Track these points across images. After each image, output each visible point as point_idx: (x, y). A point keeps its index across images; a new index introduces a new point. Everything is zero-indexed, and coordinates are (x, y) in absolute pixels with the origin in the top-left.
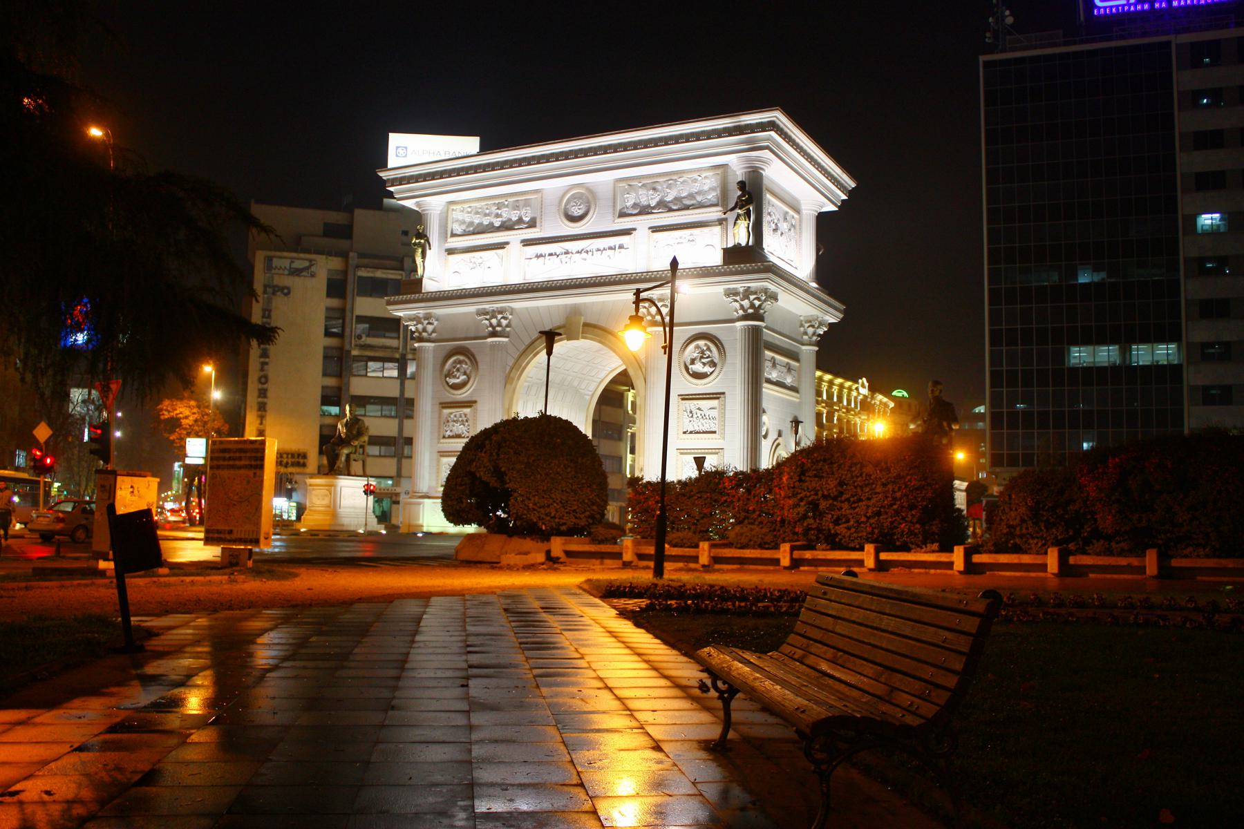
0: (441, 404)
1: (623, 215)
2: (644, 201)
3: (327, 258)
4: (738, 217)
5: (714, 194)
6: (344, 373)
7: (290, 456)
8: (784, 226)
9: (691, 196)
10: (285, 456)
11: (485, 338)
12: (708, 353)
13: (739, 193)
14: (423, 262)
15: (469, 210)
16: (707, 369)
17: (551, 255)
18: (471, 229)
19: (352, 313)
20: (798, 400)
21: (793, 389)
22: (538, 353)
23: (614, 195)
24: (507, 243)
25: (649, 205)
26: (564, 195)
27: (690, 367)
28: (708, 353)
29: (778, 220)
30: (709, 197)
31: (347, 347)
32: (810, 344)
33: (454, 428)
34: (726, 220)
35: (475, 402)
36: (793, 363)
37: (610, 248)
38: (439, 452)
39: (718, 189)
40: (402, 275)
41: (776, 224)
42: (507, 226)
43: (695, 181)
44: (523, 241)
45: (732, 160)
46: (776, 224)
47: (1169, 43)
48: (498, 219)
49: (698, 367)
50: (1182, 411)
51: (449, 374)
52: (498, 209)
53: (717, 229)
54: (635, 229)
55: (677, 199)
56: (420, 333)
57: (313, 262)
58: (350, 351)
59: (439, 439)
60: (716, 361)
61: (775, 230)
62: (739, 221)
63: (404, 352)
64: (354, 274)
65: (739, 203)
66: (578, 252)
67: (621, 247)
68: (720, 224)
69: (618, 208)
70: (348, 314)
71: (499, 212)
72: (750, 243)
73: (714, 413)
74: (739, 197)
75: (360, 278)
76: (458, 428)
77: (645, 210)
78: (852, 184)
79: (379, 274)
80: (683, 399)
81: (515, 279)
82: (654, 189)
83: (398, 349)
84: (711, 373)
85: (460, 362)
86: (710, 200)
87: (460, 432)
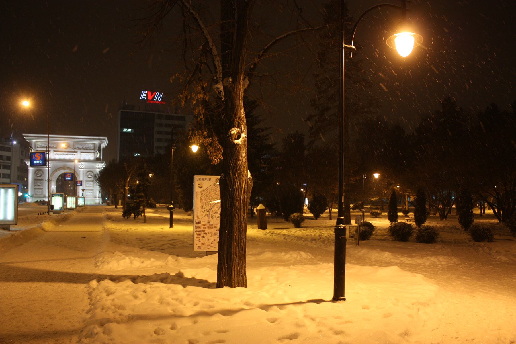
1: (75, 149)
2: (79, 147)
4: (98, 153)
9: (88, 147)
16: (91, 177)
18: (42, 147)
43: (89, 145)
45: (97, 143)
49: (89, 176)
51: (37, 174)
53: (93, 154)
55: (86, 148)
69: (74, 147)
73: (92, 184)
76: (39, 184)
77: (79, 149)
82: (81, 145)
85: (39, 172)
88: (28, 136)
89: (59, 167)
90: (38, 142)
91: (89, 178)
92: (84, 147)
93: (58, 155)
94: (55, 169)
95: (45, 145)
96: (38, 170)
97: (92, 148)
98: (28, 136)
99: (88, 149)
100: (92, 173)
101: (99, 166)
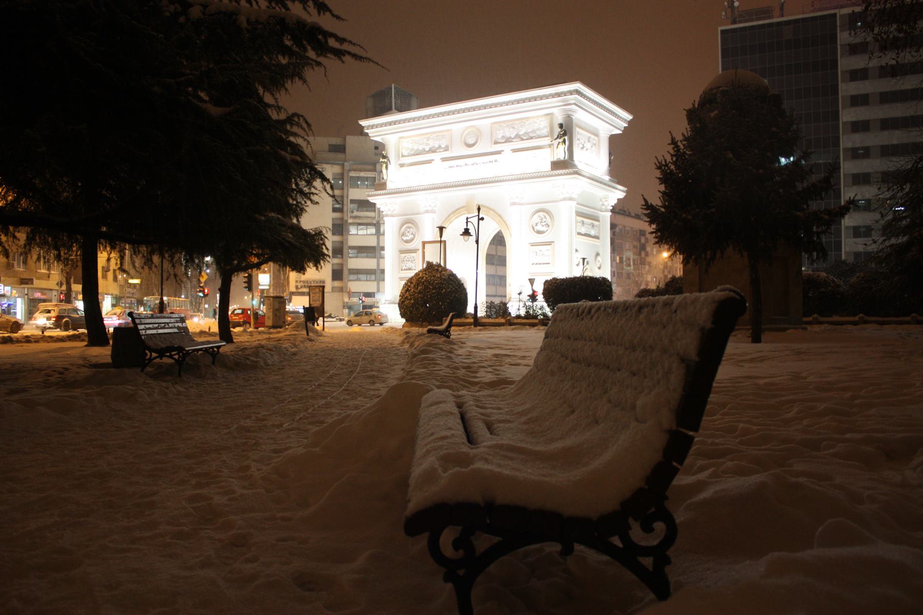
0: (400, 251)
1: (496, 143)
2: (508, 135)
3: (332, 167)
4: (559, 143)
5: (546, 130)
6: (344, 233)
7: (315, 282)
8: (588, 145)
9: (534, 131)
10: (312, 282)
11: (423, 214)
12: (544, 220)
13: (560, 130)
14: (387, 172)
15: (412, 141)
17: (457, 166)
18: (413, 152)
19: (348, 198)
20: (599, 244)
21: (597, 237)
22: (452, 221)
23: (491, 133)
24: (433, 160)
25: (511, 137)
26: (463, 132)
27: (535, 227)
28: (544, 220)
29: (584, 142)
30: (544, 132)
31: (345, 218)
32: (606, 211)
33: (407, 265)
34: (553, 144)
35: (418, 250)
36: (595, 223)
37: (490, 162)
38: (399, 278)
39: (548, 127)
40: (375, 175)
41: (583, 145)
42: (432, 151)
44: (441, 159)
46: (583, 145)
47: (834, 15)
48: (428, 147)
49: (539, 228)
50: (841, 242)
51: (403, 235)
52: (427, 140)
53: (549, 149)
54: (503, 151)
55: (526, 133)
56: (387, 212)
57: (324, 169)
58: (347, 221)
59: (399, 271)
60: (549, 224)
61: (582, 148)
62: (559, 146)
63: (379, 220)
64: (348, 176)
65: (559, 136)
67: (496, 161)
68: (550, 147)
70: (345, 199)
71: (428, 142)
72: (566, 158)
74: (559, 133)
75: (351, 177)
76: (409, 265)
77: (508, 140)
78: (629, 117)
79: (362, 174)
80: (532, 245)
81: (438, 181)
82: (513, 128)
83: (375, 218)
84: (547, 231)
85: (409, 228)
86: (544, 133)
87: (411, 267)
88: (377, 126)
89: (457, 207)
90: (403, 140)
91: (539, 232)
92: (521, 133)
93: (452, 168)
95: (423, 144)
96: (413, 224)
97: (546, 134)
98: (377, 126)
99: (532, 135)
100: (547, 217)
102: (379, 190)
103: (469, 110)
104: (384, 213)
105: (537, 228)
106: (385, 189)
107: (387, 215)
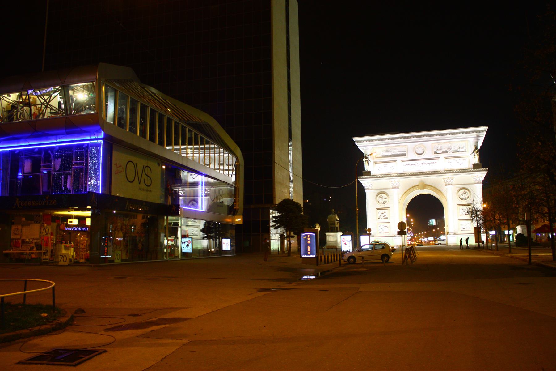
1: (436, 153)
4: (475, 155)
22: (410, 193)
26: (415, 147)
37: (432, 163)
54: (439, 158)
62: (475, 157)
66: (421, 164)
67: (435, 163)
81: (401, 171)
88: (361, 141)
89: (413, 186)
94: (406, 190)
98: (361, 141)
100: (467, 191)
101: (480, 177)
102: (366, 176)
103: (417, 136)
104: (365, 188)
105: (462, 197)
106: (370, 175)
107: (368, 189)
